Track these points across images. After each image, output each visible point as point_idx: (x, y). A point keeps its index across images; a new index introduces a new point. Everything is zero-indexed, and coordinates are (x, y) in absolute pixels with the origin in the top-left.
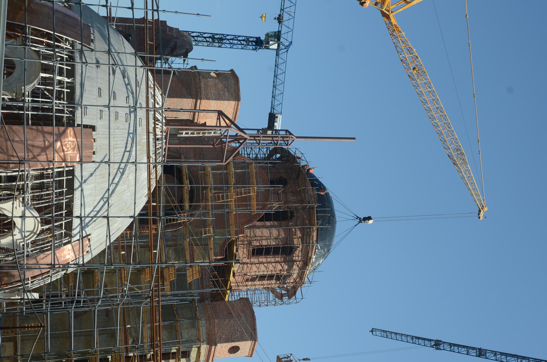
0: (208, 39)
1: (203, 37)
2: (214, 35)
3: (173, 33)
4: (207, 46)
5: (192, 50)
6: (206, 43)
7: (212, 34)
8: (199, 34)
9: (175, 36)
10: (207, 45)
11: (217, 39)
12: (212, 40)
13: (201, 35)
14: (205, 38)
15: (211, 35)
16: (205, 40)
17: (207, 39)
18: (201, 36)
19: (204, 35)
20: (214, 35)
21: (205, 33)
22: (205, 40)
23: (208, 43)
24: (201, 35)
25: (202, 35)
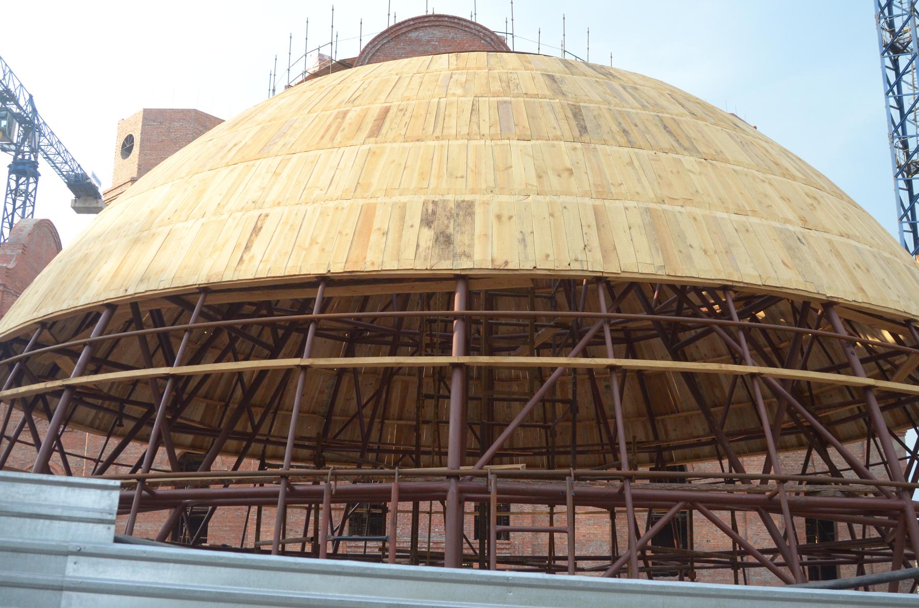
0: (18, 203)
1: (13, 214)
2: (11, 190)
3: (12, 256)
4: (33, 206)
5: (52, 223)
6: (27, 208)
7: (7, 195)
8: (6, 220)
9: (20, 251)
10: (32, 207)
11: (18, 185)
12: (21, 195)
13: (7, 217)
14: (14, 210)
15: (10, 196)
16: (19, 211)
17: (16, 207)
18: (10, 217)
19: (10, 210)
20: (11, 190)
21: (5, 209)
22: (19, 211)
23: (28, 203)
24: (7, 217)
25: (8, 216)
